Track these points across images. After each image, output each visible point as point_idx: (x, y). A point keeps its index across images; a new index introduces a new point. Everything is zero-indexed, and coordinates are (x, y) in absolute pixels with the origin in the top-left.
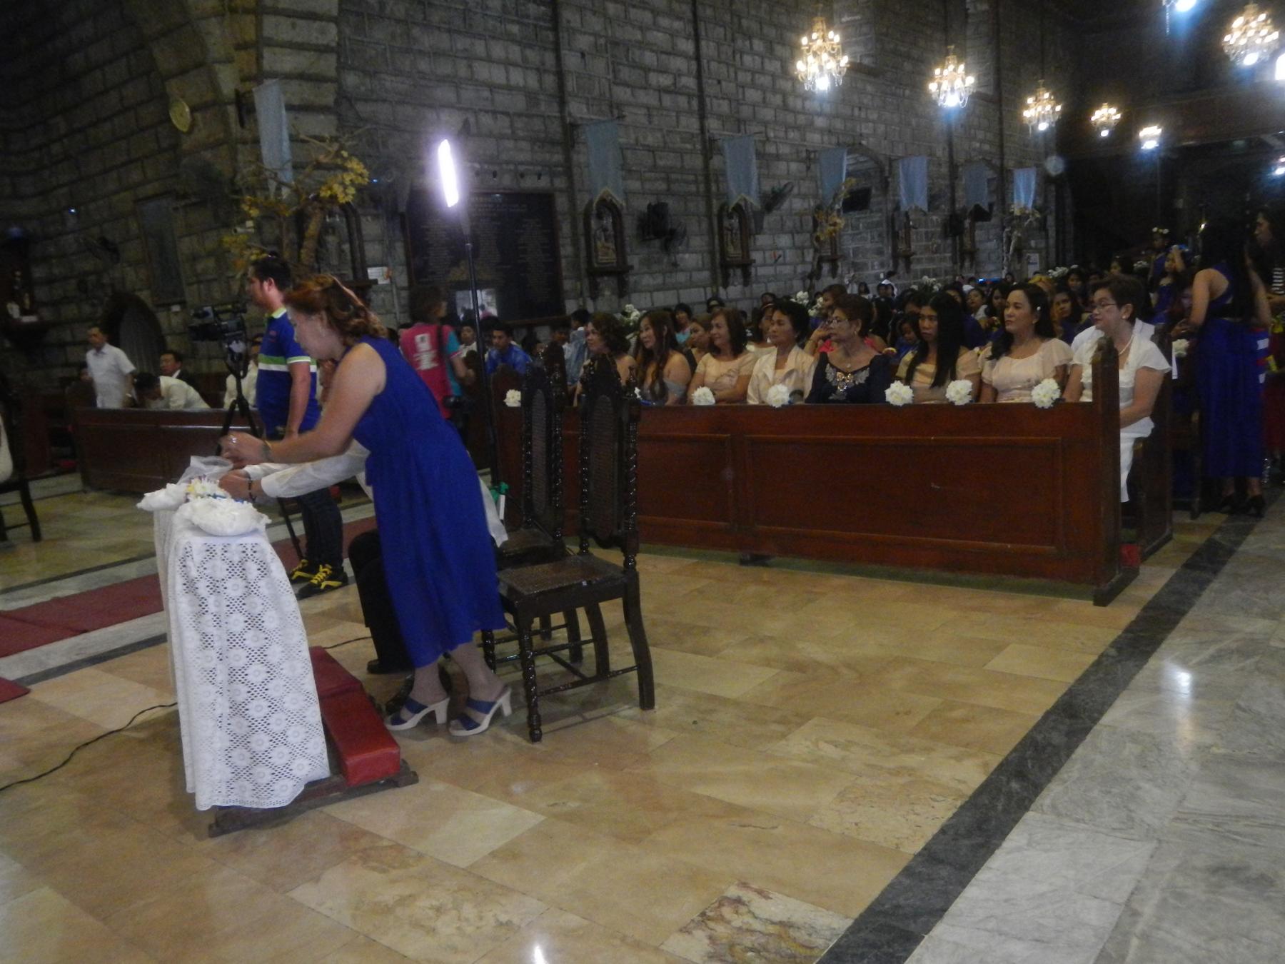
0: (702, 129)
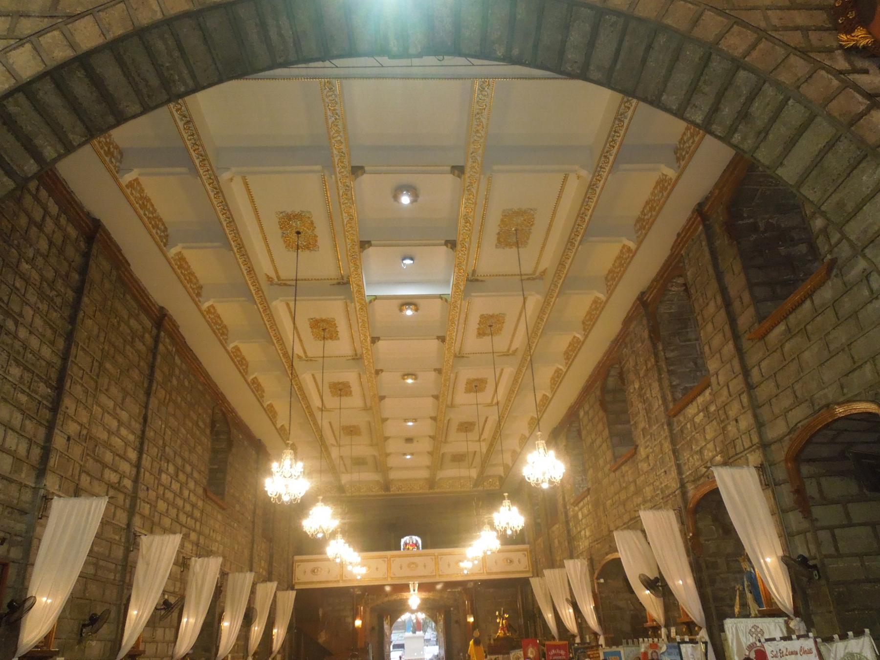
0: (129, 525)
